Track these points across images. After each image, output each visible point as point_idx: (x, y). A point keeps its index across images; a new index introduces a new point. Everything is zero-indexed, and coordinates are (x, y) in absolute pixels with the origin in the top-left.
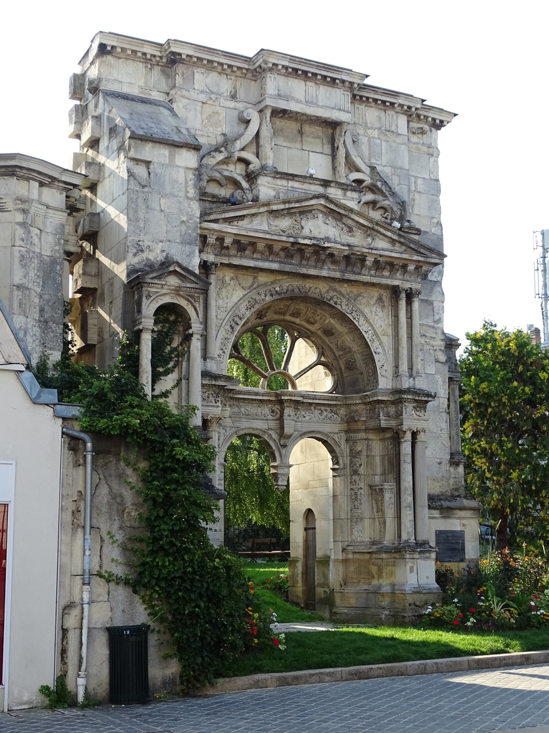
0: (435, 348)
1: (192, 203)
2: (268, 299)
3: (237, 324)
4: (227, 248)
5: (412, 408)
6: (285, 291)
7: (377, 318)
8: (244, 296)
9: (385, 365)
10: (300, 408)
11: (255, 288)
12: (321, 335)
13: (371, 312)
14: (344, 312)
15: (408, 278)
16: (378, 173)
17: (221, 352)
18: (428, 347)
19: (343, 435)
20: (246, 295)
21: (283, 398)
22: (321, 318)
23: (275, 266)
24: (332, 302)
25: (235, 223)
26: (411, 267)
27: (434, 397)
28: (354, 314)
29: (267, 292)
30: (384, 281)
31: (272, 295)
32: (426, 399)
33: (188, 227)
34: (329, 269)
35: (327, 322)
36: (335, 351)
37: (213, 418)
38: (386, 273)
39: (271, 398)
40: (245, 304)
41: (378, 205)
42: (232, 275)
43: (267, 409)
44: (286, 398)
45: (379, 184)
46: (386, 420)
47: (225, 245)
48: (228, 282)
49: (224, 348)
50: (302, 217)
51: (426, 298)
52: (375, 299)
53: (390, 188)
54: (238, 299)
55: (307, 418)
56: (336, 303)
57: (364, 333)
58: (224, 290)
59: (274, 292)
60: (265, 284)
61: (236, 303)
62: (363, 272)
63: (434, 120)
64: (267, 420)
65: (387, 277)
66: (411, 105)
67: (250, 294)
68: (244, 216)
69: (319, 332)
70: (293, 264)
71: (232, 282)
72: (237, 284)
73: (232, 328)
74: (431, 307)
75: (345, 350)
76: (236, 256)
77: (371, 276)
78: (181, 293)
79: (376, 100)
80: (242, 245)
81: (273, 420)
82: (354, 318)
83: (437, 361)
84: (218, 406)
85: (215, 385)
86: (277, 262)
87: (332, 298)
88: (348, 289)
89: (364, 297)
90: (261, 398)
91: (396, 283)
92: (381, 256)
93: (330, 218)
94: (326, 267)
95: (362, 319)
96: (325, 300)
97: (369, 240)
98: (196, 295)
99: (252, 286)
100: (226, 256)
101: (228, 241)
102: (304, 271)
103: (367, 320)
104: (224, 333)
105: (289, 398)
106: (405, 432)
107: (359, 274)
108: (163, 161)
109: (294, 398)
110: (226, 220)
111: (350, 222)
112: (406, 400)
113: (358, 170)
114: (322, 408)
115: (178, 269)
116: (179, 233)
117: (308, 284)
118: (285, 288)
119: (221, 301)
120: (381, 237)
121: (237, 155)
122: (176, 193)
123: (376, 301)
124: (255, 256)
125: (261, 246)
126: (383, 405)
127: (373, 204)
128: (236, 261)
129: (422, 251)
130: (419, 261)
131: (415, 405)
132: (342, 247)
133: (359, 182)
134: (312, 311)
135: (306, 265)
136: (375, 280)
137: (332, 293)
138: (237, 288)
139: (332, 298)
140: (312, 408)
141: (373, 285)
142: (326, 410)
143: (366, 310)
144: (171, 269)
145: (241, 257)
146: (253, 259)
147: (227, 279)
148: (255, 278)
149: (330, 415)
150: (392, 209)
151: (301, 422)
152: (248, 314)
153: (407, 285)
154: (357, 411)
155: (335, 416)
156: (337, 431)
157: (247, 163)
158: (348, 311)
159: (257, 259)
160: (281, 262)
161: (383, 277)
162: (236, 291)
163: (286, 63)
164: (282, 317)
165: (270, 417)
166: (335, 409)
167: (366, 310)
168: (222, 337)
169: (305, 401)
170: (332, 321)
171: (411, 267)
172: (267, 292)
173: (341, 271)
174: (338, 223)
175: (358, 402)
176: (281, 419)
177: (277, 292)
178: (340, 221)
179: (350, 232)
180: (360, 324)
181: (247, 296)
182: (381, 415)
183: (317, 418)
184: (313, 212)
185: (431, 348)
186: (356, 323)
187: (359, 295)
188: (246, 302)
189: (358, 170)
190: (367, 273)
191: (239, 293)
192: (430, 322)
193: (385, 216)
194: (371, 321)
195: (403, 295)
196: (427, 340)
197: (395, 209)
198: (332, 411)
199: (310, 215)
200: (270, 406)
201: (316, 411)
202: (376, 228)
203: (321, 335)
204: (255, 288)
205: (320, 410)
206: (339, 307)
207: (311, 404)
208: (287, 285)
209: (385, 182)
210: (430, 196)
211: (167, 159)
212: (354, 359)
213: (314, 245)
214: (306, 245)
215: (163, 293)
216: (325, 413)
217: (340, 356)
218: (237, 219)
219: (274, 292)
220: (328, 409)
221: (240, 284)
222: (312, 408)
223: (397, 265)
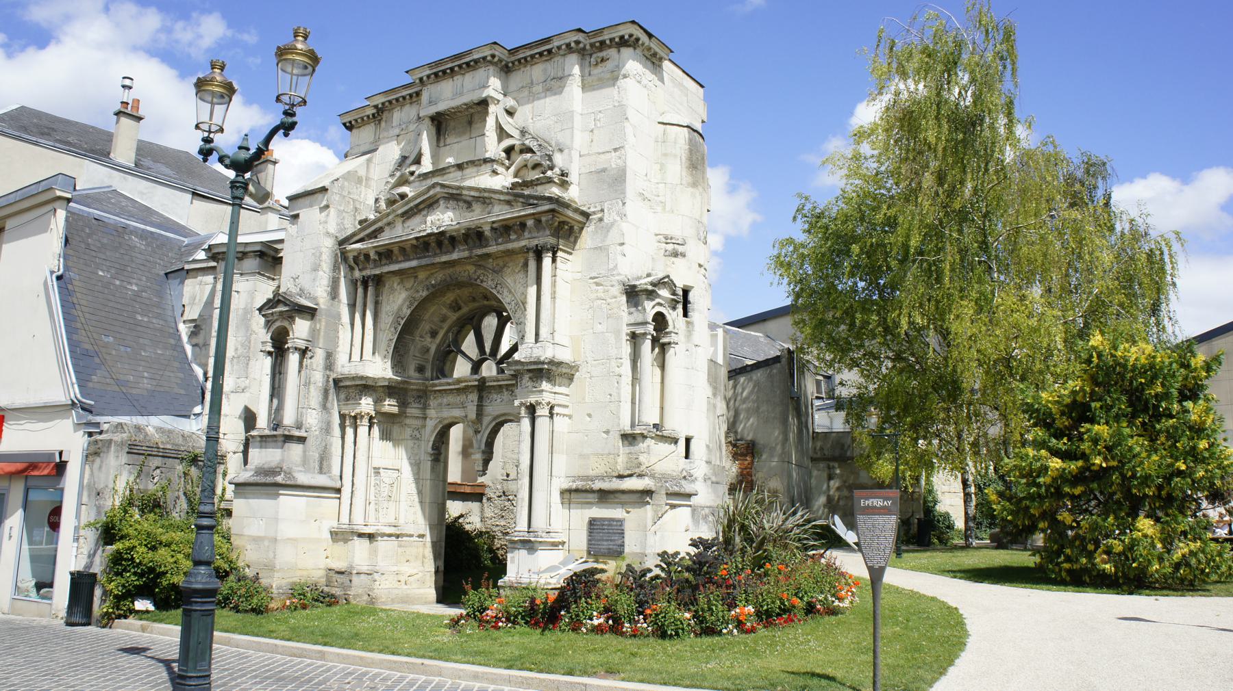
0: (609, 300)
2: (425, 294)
63: (612, 40)
66: (567, 41)
79: (532, 56)
101: (373, 255)
103: (510, 292)
117: (458, 269)
125: (396, 250)
137: (479, 272)
152: (409, 312)
153: (535, 242)
161: (510, 241)
163: (428, 72)
171: (530, 223)
191: (404, 295)
195: (531, 254)
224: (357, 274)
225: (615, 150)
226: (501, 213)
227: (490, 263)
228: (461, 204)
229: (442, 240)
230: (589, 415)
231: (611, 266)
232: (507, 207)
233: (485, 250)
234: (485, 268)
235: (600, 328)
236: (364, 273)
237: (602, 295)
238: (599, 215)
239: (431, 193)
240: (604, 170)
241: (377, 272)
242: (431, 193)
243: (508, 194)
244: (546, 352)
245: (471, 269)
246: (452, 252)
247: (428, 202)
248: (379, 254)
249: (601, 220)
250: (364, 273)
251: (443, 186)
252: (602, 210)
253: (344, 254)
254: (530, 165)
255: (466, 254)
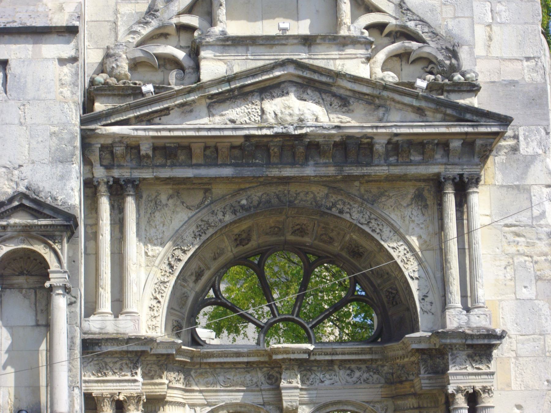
0: (536, 258)
1: (66, 106)
2: (228, 218)
3: (180, 260)
4: (147, 156)
5: (464, 357)
6: (255, 203)
7: (412, 225)
8: (190, 218)
9: (430, 295)
10: (315, 368)
11: (207, 206)
12: (348, 257)
13: (403, 218)
14: (355, 222)
15: (456, 160)
16: (408, 9)
17: (154, 302)
18: (523, 259)
19: (390, 403)
20: (192, 216)
21: (274, 357)
22: (339, 234)
23: (227, 171)
24: (334, 211)
25: (157, 120)
26: (456, 144)
27: (501, 337)
28: (373, 223)
29: (227, 208)
30: (412, 170)
31: (234, 212)
32: (486, 341)
33: (61, 140)
34: (316, 164)
35: (347, 238)
36: (372, 279)
37: (129, 398)
38: (416, 158)
39: (262, 359)
40: (191, 230)
41: (413, 57)
42: (171, 192)
43: (260, 375)
44: (280, 357)
45: (411, 25)
46: (429, 379)
47: (143, 152)
48: (164, 202)
49: (159, 296)
50: (263, 96)
51: (517, 183)
52: (410, 196)
53: (429, 26)
54: (182, 223)
55: (327, 382)
56: (341, 212)
57: (391, 251)
58: (157, 214)
59: (238, 208)
60: (223, 198)
61: (177, 231)
62: (376, 161)
64: (261, 390)
65: (419, 163)
67: (199, 215)
68: (167, 109)
69: (344, 254)
70: (256, 165)
71: (171, 202)
72: (179, 203)
73: (171, 267)
74: (526, 196)
75: (382, 276)
76: (163, 166)
77: (389, 165)
78: (34, 233)
80: (171, 151)
81: (269, 390)
82: (374, 231)
83: (539, 278)
84: (135, 381)
85: (127, 352)
86: (231, 165)
87: (334, 205)
88: (362, 191)
89: (390, 197)
90: (245, 359)
91: (434, 169)
92: (396, 135)
93: (309, 91)
94: (311, 163)
95: (386, 231)
96: (323, 209)
97: (381, 112)
98: (57, 233)
99: (202, 202)
100: (148, 167)
101: (145, 149)
102: (275, 172)
104: (159, 275)
105: (285, 356)
106: (453, 395)
107: (369, 164)
108: (23, 57)
109: (292, 356)
110: (139, 120)
111: (342, 92)
112: (451, 347)
113: (378, 10)
114: (353, 366)
115: (26, 203)
116: (47, 150)
117: (293, 189)
118: (256, 199)
119: (153, 231)
120: (398, 106)
121: (175, 21)
122: (43, 96)
123: (412, 199)
124: (194, 161)
126: (425, 357)
127: (403, 56)
128: (166, 173)
129: (468, 116)
130: (467, 134)
131: (470, 351)
132: (325, 132)
133: (379, 27)
134: (322, 225)
135: (277, 164)
136: (397, 170)
137: (334, 198)
138: (178, 209)
139: (334, 205)
140: (336, 367)
141: (403, 178)
142: (359, 369)
143: (394, 217)
144: (16, 203)
145: (173, 166)
146: (191, 166)
147: (163, 198)
148: (207, 191)
149: (365, 375)
150: (437, 58)
151: (316, 389)
153: (455, 171)
154: (403, 367)
155: (376, 376)
156: (378, 398)
157: (191, 29)
158: (363, 221)
159: (198, 166)
160: (235, 165)
161: (411, 163)
162: (178, 213)
164: (282, 238)
165: (266, 386)
166: (374, 366)
167: (393, 216)
168: (156, 281)
169: (318, 358)
170: (354, 237)
171: (456, 144)
172: (227, 208)
173: (336, 165)
174: (324, 96)
175: (401, 353)
176: (278, 390)
177: (242, 207)
178: (326, 92)
179: (345, 105)
180: (384, 237)
181: (194, 218)
182: (422, 372)
183: (344, 382)
184: (282, 86)
185: (530, 259)
186: (377, 237)
187: (382, 194)
188: (194, 228)
189: (378, 10)
190: (382, 162)
192: (524, 218)
193: (428, 70)
194: (401, 230)
196: (520, 248)
197: (440, 57)
198: (369, 369)
199: (276, 92)
200: (265, 369)
201: (341, 372)
202: (385, 93)
203: (348, 257)
204: (207, 206)
205: (349, 368)
206: (347, 217)
207: (331, 362)
208: (259, 194)
209: (421, 20)
210: (520, 26)
211: (30, 53)
212: (397, 290)
213: (277, 135)
214: (266, 136)
215: (7, 236)
216: (357, 374)
217: (379, 286)
218: (156, 115)
219: (238, 208)
220: (363, 367)
221: (183, 203)
222: (336, 367)
223: (428, 143)
224: (100, 173)
225: (528, 59)
226: (402, 124)
227: (355, 188)
228: (328, 98)
229: (295, 146)
230: (519, 407)
231: (536, 212)
232: (413, 116)
233: (365, 170)
234: (348, 195)
235: (525, 293)
236: (116, 173)
237: (522, 248)
238: (512, 142)
239: (277, 73)
240: (517, 82)
241: (138, 174)
242: (277, 73)
243: (425, 98)
244: (478, 321)
245: (320, 192)
246: (304, 164)
247: (262, 85)
248: (155, 149)
249: (515, 149)
250: (116, 173)
251: (299, 65)
252: (516, 137)
253: (87, 139)
254: (413, 57)
255: (331, 171)
